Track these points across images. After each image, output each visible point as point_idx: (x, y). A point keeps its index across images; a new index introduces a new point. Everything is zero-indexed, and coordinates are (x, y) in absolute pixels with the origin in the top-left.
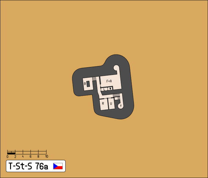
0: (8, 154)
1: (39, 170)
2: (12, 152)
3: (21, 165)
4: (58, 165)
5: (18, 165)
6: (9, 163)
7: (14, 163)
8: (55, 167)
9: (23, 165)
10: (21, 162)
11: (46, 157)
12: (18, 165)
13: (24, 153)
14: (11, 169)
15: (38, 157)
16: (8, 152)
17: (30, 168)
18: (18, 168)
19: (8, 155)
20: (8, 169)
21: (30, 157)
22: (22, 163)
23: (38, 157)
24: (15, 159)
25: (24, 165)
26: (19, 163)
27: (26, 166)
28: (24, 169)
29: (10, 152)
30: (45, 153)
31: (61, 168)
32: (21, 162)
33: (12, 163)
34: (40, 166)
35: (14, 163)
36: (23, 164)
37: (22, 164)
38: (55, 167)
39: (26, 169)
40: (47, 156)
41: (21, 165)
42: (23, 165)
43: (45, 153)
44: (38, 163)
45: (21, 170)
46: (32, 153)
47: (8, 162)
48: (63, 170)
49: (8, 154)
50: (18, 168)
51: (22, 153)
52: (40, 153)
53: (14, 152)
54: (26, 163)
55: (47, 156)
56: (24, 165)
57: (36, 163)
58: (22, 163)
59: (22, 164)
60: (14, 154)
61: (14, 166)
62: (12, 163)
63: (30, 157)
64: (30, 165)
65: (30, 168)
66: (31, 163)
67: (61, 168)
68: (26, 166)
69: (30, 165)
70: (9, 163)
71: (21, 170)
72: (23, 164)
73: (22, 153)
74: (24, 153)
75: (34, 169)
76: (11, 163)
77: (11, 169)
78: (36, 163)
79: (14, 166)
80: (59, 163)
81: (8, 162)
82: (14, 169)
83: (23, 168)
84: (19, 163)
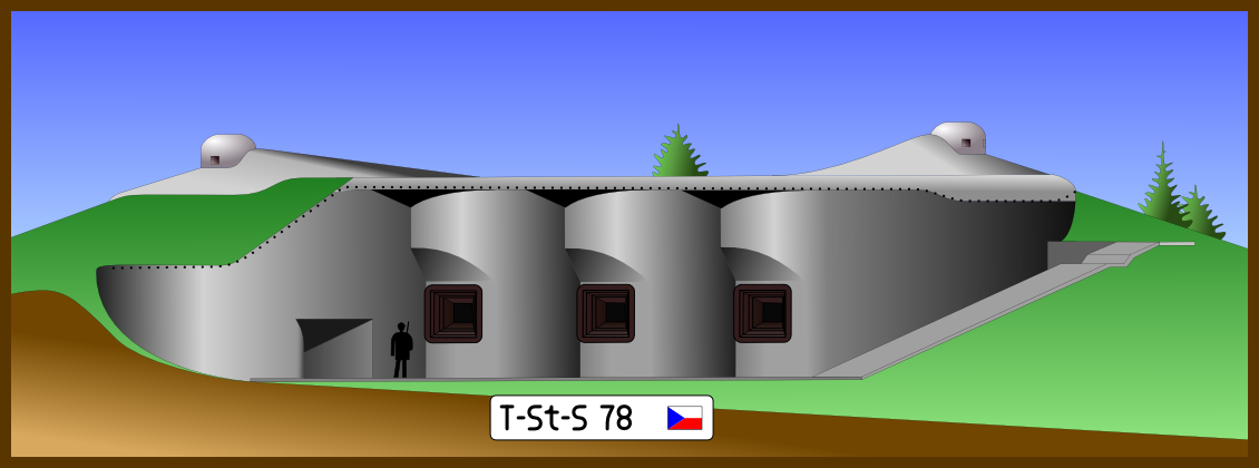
1: (615, 433)
3: (548, 416)
5: (534, 412)
7: (521, 405)
8: (674, 420)
9: (555, 416)
10: (546, 402)
12: (534, 412)
14: (507, 428)
17: (581, 423)
18: (536, 423)
20: (498, 432)
22: (551, 407)
25: (557, 412)
26: (540, 407)
27: (563, 418)
28: (557, 429)
32: (546, 402)
33: (512, 407)
34: (621, 417)
35: (521, 405)
36: (555, 409)
37: (551, 412)
38: (674, 420)
39: (566, 431)
41: (548, 416)
42: (555, 416)
44: (612, 407)
50: (536, 423)
54: (564, 405)
56: (557, 412)
57: (602, 407)
58: (551, 407)
59: (551, 412)
61: (519, 418)
62: (512, 407)
64: (579, 412)
65: (581, 423)
66: (585, 407)
68: (563, 418)
69: (579, 412)
71: (546, 433)
72: (555, 409)
75: (595, 431)
76: (507, 408)
77: (507, 428)
78: (602, 407)
79: (519, 418)
82: (520, 431)
83: (555, 425)
84: (540, 407)
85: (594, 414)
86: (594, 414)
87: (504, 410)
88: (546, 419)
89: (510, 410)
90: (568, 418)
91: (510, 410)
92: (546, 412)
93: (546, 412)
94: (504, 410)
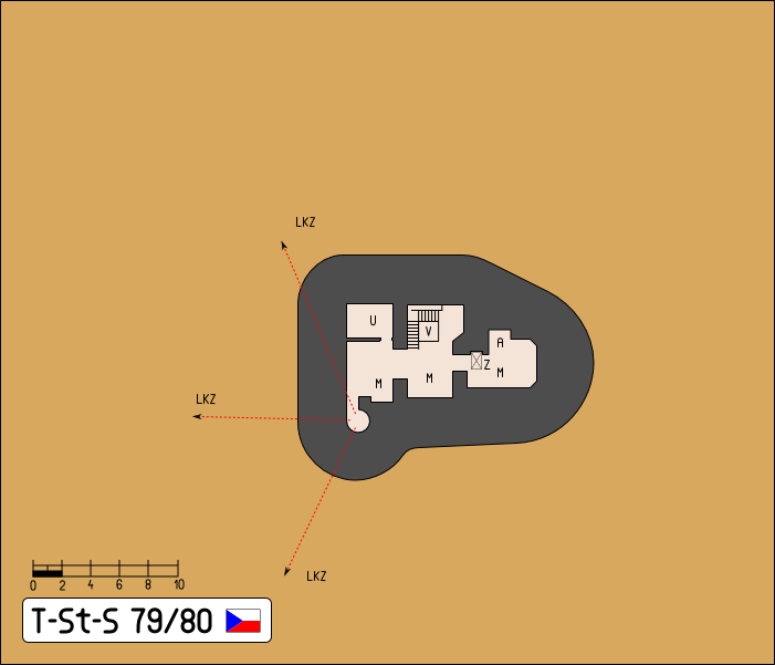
0: (36, 574)
1: (145, 635)
2: (51, 569)
3: (80, 618)
4: (244, 616)
5: (65, 615)
6: (33, 610)
7: (52, 607)
9: (86, 618)
10: (78, 605)
11: (178, 586)
12: (65, 615)
13: (96, 571)
14: (39, 632)
15: (148, 585)
16: (36, 569)
17: (111, 626)
18: (67, 626)
19: (35, 579)
20: (30, 634)
21: (119, 586)
22: (83, 610)
23: (148, 585)
24: (62, 594)
25: (88, 615)
26: (72, 610)
27: (94, 621)
28: (88, 632)
29: (44, 569)
30: (173, 571)
31: (254, 627)
32: (78, 605)
33: (44, 610)
34: (159, 620)
35: (52, 607)
36: (86, 612)
37: (83, 615)
38: (233, 623)
39: (97, 632)
40: (179, 584)
41: (80, 618)
42: (86, 618)
43: (173, 571)
44: (142, 610)
45: (77, 635)
46: (125, 571)
47: (30, 604)
48: (264, 635)
49: (36, 574)
50: (67, 626)
51: (86, 571)
52: (153, 571)
53: (59, 569)
54: (95, 608)
55: (179, 584)
56: (88, 615)
57: (133, 610)
58: (83, 610)
59: (83, 615)
60: (59, 574)
61: (50, 621)
62: (44, 610)
63: (119, 586)
64: (110, 615)
65: (111, 626)
66: (116, 610)
67: (254, 627)
68: (94, 621)
69: (110, 615)
70: (33, 610)
71: (77, 635)
72: (86, 612)
73: (86, 571)
74: (96, 571)
75: (126, 633)
76: (39, 611)
77: (39, 632)
78: (133, 610)
79: (50, 621)
80: (246, 610)
81: (30, 604)
82: (51, 633)
83: (86, 628)
84: (72, 610)
85: (125, 617)
86: (125, 617)
87: (36, 613)
88: (77, 622)
89: (42, 613)
90: (99, 621)
91: (42, 613)
92: (77, 615)
93: (77, 615)
94: (36, 613)
